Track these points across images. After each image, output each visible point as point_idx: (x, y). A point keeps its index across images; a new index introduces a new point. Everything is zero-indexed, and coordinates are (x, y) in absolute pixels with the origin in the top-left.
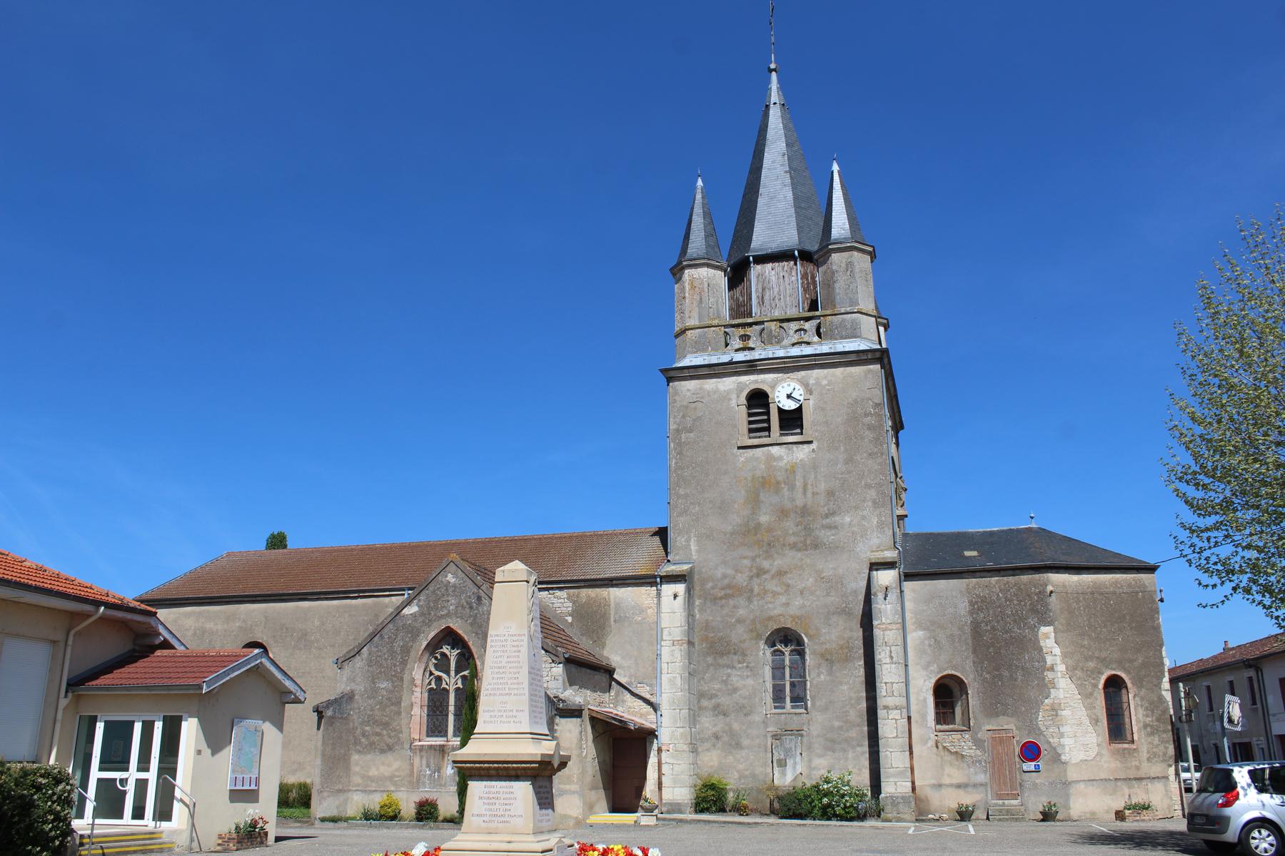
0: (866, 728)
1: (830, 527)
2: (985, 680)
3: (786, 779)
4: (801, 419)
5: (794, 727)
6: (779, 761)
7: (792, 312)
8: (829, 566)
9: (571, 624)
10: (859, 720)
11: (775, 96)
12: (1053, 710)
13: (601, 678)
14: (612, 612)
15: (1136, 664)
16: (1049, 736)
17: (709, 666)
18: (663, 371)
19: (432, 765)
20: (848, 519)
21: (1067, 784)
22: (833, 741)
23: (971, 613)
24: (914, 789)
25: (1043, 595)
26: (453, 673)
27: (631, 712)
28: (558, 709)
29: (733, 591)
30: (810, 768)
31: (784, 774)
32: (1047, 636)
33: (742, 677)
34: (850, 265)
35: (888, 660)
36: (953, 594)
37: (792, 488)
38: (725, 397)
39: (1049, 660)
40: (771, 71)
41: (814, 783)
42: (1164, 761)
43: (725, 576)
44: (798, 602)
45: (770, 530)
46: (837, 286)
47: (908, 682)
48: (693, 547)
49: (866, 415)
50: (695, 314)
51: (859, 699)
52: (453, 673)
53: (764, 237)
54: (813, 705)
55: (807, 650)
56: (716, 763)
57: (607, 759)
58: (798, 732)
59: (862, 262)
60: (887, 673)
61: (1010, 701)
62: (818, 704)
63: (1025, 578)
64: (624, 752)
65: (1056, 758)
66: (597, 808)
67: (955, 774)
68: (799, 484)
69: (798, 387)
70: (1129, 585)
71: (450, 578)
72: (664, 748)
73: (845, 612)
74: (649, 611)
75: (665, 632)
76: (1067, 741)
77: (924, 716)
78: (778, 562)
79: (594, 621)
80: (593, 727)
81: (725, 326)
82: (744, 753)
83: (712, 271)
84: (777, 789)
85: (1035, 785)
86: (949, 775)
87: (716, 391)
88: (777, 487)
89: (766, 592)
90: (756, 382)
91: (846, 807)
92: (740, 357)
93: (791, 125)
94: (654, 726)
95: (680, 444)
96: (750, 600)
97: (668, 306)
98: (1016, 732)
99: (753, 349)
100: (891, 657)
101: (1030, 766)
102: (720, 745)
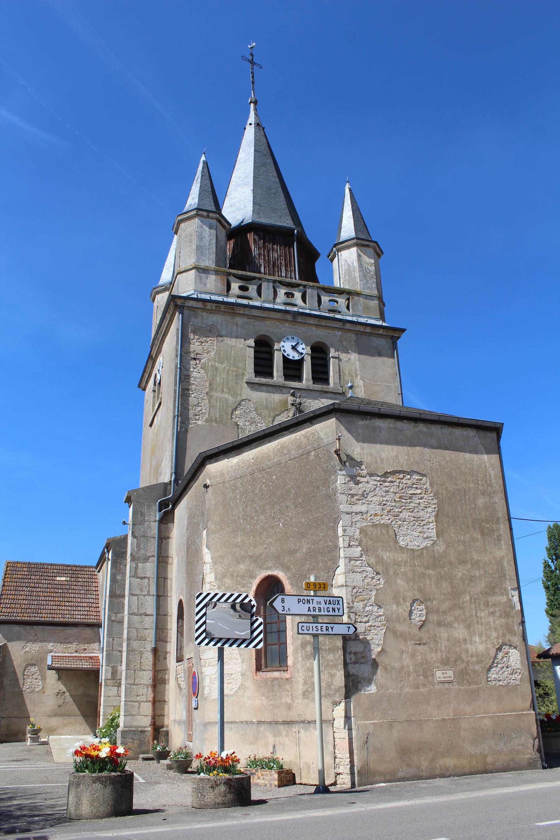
15: (299, 555)
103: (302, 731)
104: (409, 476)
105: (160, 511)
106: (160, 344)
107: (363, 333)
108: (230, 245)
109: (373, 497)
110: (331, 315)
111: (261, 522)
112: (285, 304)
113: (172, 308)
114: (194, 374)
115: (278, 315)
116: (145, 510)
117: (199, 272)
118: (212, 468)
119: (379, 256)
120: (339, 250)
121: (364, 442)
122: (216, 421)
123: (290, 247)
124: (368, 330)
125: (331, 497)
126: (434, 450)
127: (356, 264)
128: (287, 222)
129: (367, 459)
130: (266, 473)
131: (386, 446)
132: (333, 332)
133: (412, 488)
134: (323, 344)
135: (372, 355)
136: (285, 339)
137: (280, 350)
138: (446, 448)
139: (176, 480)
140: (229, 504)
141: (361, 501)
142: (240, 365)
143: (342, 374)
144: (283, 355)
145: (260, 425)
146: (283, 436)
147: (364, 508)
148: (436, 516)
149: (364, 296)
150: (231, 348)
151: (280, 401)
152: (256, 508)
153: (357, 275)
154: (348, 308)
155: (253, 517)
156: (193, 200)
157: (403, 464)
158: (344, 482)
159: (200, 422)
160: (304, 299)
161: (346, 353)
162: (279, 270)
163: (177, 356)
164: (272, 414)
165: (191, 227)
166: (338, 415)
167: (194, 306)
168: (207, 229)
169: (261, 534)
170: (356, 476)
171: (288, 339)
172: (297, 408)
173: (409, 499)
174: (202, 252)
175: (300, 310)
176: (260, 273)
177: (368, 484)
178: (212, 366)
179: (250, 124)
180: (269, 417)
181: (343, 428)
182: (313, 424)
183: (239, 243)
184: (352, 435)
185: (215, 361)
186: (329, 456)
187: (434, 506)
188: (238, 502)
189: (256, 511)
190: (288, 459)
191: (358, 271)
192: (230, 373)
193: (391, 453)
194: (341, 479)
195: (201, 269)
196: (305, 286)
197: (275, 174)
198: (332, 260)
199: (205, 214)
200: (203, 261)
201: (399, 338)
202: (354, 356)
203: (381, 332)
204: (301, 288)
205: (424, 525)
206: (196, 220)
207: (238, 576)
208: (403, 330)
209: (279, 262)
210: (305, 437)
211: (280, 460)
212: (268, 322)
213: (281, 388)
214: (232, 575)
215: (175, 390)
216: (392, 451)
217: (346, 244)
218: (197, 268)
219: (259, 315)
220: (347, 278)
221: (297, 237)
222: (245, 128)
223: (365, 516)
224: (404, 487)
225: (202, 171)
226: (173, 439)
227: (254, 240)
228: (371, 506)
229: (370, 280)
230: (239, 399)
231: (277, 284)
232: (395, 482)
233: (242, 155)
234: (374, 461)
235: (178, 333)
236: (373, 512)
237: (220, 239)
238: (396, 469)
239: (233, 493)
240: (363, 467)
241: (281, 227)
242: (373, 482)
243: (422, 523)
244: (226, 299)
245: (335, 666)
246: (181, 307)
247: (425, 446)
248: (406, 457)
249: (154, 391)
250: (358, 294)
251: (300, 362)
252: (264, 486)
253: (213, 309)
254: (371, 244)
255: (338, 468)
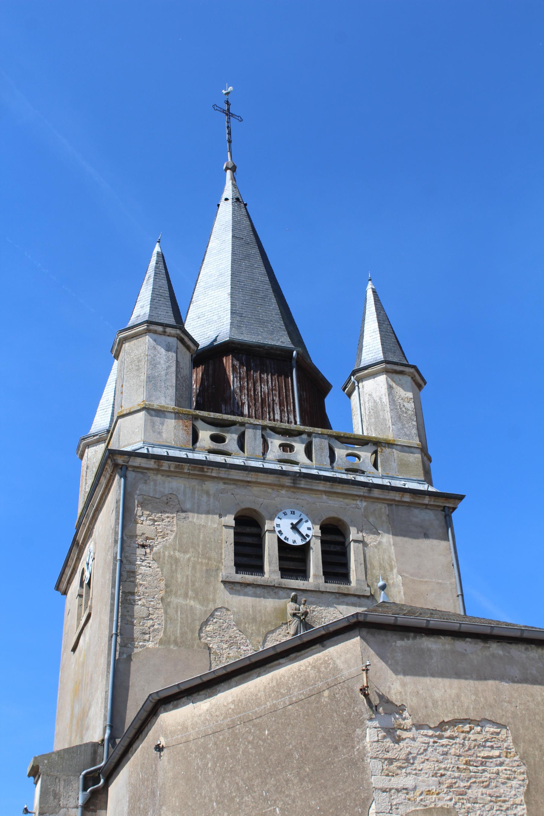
104: (479, 729)
105: (85, 789)
106: (90, 523)
107: (400, 503)
108: (197, 374)
109: (423, 762)
110: (350, 477)
111: (246, 806)
112: (281, 461)
113: (109, 469)
114: (143, 570)
115: (271, 479)
116: (61, 788)
117: (151, 415)
118: (168, 718)
119: (420, 387)
120: (359, 380)
121: (405, 674)
122: (176, 643)
123: (286, 377)
124: (407, 498)
125: (357, 764)
126: (516, 686)
127: (386, 399)
128: (282, 340)
129: (411, 702)
130: (254, 725)
131: (440, 680)
132: (355, 502)
133: (484, 746)
134: (339, 520)
135: (414, 535)
136: (281, 514)
137: (273, 531)
138: (535, 682)
139: (112, 738)
140: (196, 778)
141: (404, 770)
142: (213, 555)
143: (368, 566)
144: (279, 539)
145: (245, 648)
146: (280, 665)
147: (409, 782)
148: (527, 793)
149: (398, 447)
150: (199, 529)
151: (275, 609)
152: (237, 784)
153: (388, 415)
154: (375, 465)
155: (232, 799)
156: (142, 309)
157: (468, 707)
158: (376, 739)
159: (150, 645)
160: (308, 452)
161: (374, 533)
162: (271, 410)
163: (116, 541)
164: (263, 630)
165: (140, 348)
166: (364, 631)
167: (143, 465)
168: (163, 351)
170: (394, 729)
171: (285, 514)
172: (301, 621)
173: (482, 764)
174: (155, 385)
175: (304, 471)
176: (242, 415)
177: (415, 741)
178: (170, 557)
179: (226, 199)
180: (258, 634)
181: (372, 652)
182: (325, 647)
183: (211, 372)
184: (386, 663)
185: (174, 550)
186: (351, 697)
187: (521, 777)
188: (210, 773)
190: (288, 703)
191: (389, 409)
192: (198, 567)
193: (449, 691)
194: (371, 734)
195: (153, 410)
196: (310, 434)
197: (263, 269)
198: (349, 395)
199: (160, 329)
200: (157, 399)
201: (454, 509)
202: (386, 539)
203: (426, 500)
204: (304, 436)
205: (507, 809)
206: (147, 339)
208: (461, 498)
209: (271, 398)
210: (314, 667)
211: (275, 705)
212: (255, 488)
213: (276, 590)
215: (113, 594)
216: (451, 687)
217: (369, 370)
218: (147, 409)
219: (241, 478)
220: (373, 420)
221: (297, 362)
222: (218, 205)
223: (411, 795)
224: (472, 745)
225: (156, 268)
226: (108, 672)
227: (233, 366)
228: (420, 778)
229: (408, 423)
230: (212, 607)
231: (269, 431)
232: (456, 737)
233: (213, 244)
234: (423, 704)
235: (117, 507)
236: (424, 788)
237: (182, 365)
238: (457, 716)
239: (201, 760)
240: (406, 714)
241: (272, 347)
242: (422, 738)
243: (505, 806)
244: (191, 456)
246: (124, 468)
247: (502, 678)
248: (473, 697)
249: (80, 596)
250: (390, 444)
251: (305, 549)
252: (250, 746)
253: (172, 469)
254: (407, 369)
255: (366, 716)
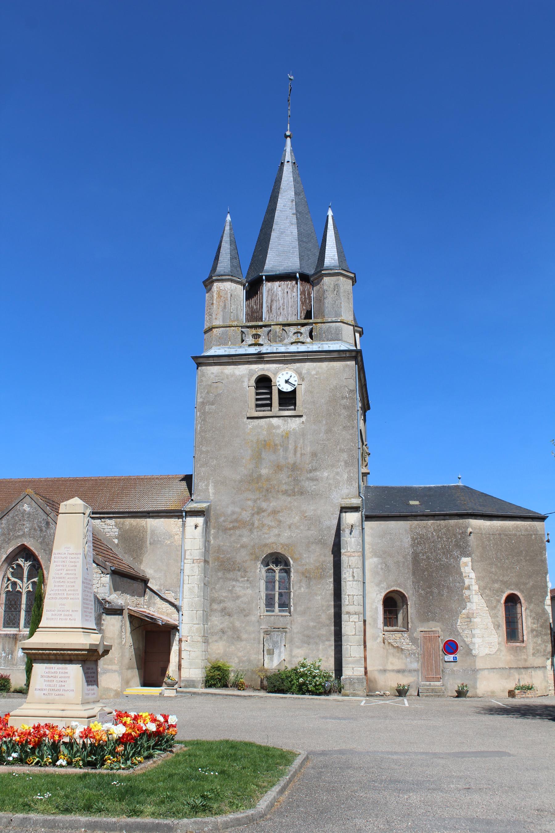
0: (333, 628)
1: (312, 479)
2: (420, 595)
3: (273, 664)
4: (295, 398)
5: (280, 626)
6: (269, 650)
7: (292, 319)
8: (310, 508)
9: (117, 545)
10: (328, 622)
11: (288, 156)
12: (468, 617)
13: (139, 586)
14: (149, 537)
15: (528, 586)
16: (464, 636)
17: (219, 579)
18: (195, 358)
19: (7, 649)
20: (326, 474)
21: (475, 671)
22: (308, 636)
23: (413, 546)
24: (366, 673)
25: (465, 535)
26: (25, 580)
27: (161, 612)
28: (104, 608)
29: (239, 524)
30: (291, 656)
31: (271, 660)
32: (466, 565)
33: (244, 588)
34: (336, 286)
35: (351, 579)
36: (400, 532)
37: (286, 449)
38: (239, 380)
39: (467, 582)
40: (286, 137)
41: (294, 667)
42: (543, 655)
43: (233, 513)
44: (287, 534)
45: (268, 480)
46: (326, 301)
47: (364, 596)
48: (211, 490)
49: (343, 398)
50: (220, 316)
51: (329, 606)
52: (25, 580)
53: (274, 262)
54: (295, 610)
55: (292, 570)
56: (222, 651)
57: (141, 646)
58: (283, 630)
59: (345, 284)
60: (350, 588)
61: (438, 610)
62: (298, 609)
63: (452, 522)
64: (153, 643)
65: (469, 652)
66: (132, 683)
67: (396, 662)
68: (291, 447)
69: (294, 375)
70: (526, 530)
71: (26, 507)
72: (183, 639)
73: (321, 542)
74: (176, 537)
75: (188, 553)
76: (477, 640)
77: (375, 620)
78: (274, 504)
79: (135, 543)
80: (131, 622)
81: (242, 327)
82: (243, 644)
83: (234, 285)
84: (266, 671)
85: (453, 671)
86: (392, 664)
87: (233, 375)
88: (274, 448)
89: (263, 525)
90: (263, 369)
91: (315, 686)
92: (253, 350)
93: (299, 179)
94: (177, 623)
95: (204, 413)
96: (251, 531)
97: (200, 309)
98: (441, 633)
99: (262, 345)
100: (353, 577)
101: (450, 657)
102: (225, 637)
103: (533, 672)
169: (507, 570)
179: (288, 162)
189: (503, 557)
207: (494, 590)
214: (490, 589)
245: (547, 642)
